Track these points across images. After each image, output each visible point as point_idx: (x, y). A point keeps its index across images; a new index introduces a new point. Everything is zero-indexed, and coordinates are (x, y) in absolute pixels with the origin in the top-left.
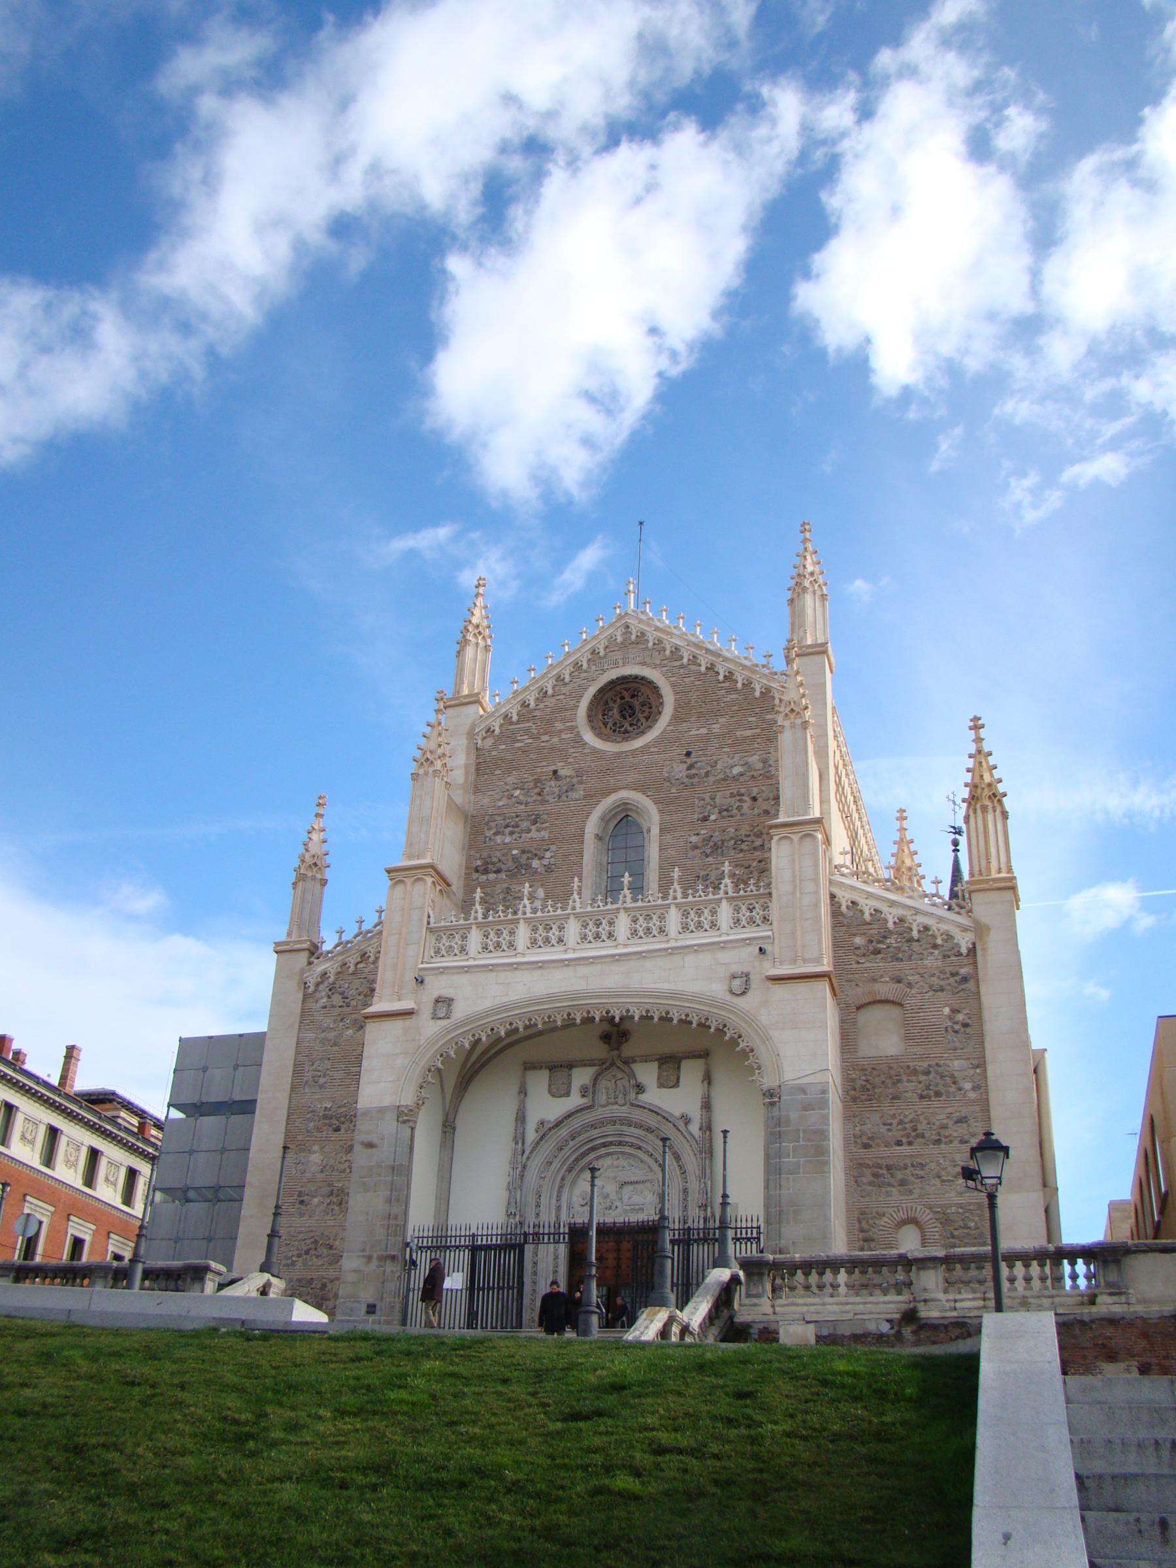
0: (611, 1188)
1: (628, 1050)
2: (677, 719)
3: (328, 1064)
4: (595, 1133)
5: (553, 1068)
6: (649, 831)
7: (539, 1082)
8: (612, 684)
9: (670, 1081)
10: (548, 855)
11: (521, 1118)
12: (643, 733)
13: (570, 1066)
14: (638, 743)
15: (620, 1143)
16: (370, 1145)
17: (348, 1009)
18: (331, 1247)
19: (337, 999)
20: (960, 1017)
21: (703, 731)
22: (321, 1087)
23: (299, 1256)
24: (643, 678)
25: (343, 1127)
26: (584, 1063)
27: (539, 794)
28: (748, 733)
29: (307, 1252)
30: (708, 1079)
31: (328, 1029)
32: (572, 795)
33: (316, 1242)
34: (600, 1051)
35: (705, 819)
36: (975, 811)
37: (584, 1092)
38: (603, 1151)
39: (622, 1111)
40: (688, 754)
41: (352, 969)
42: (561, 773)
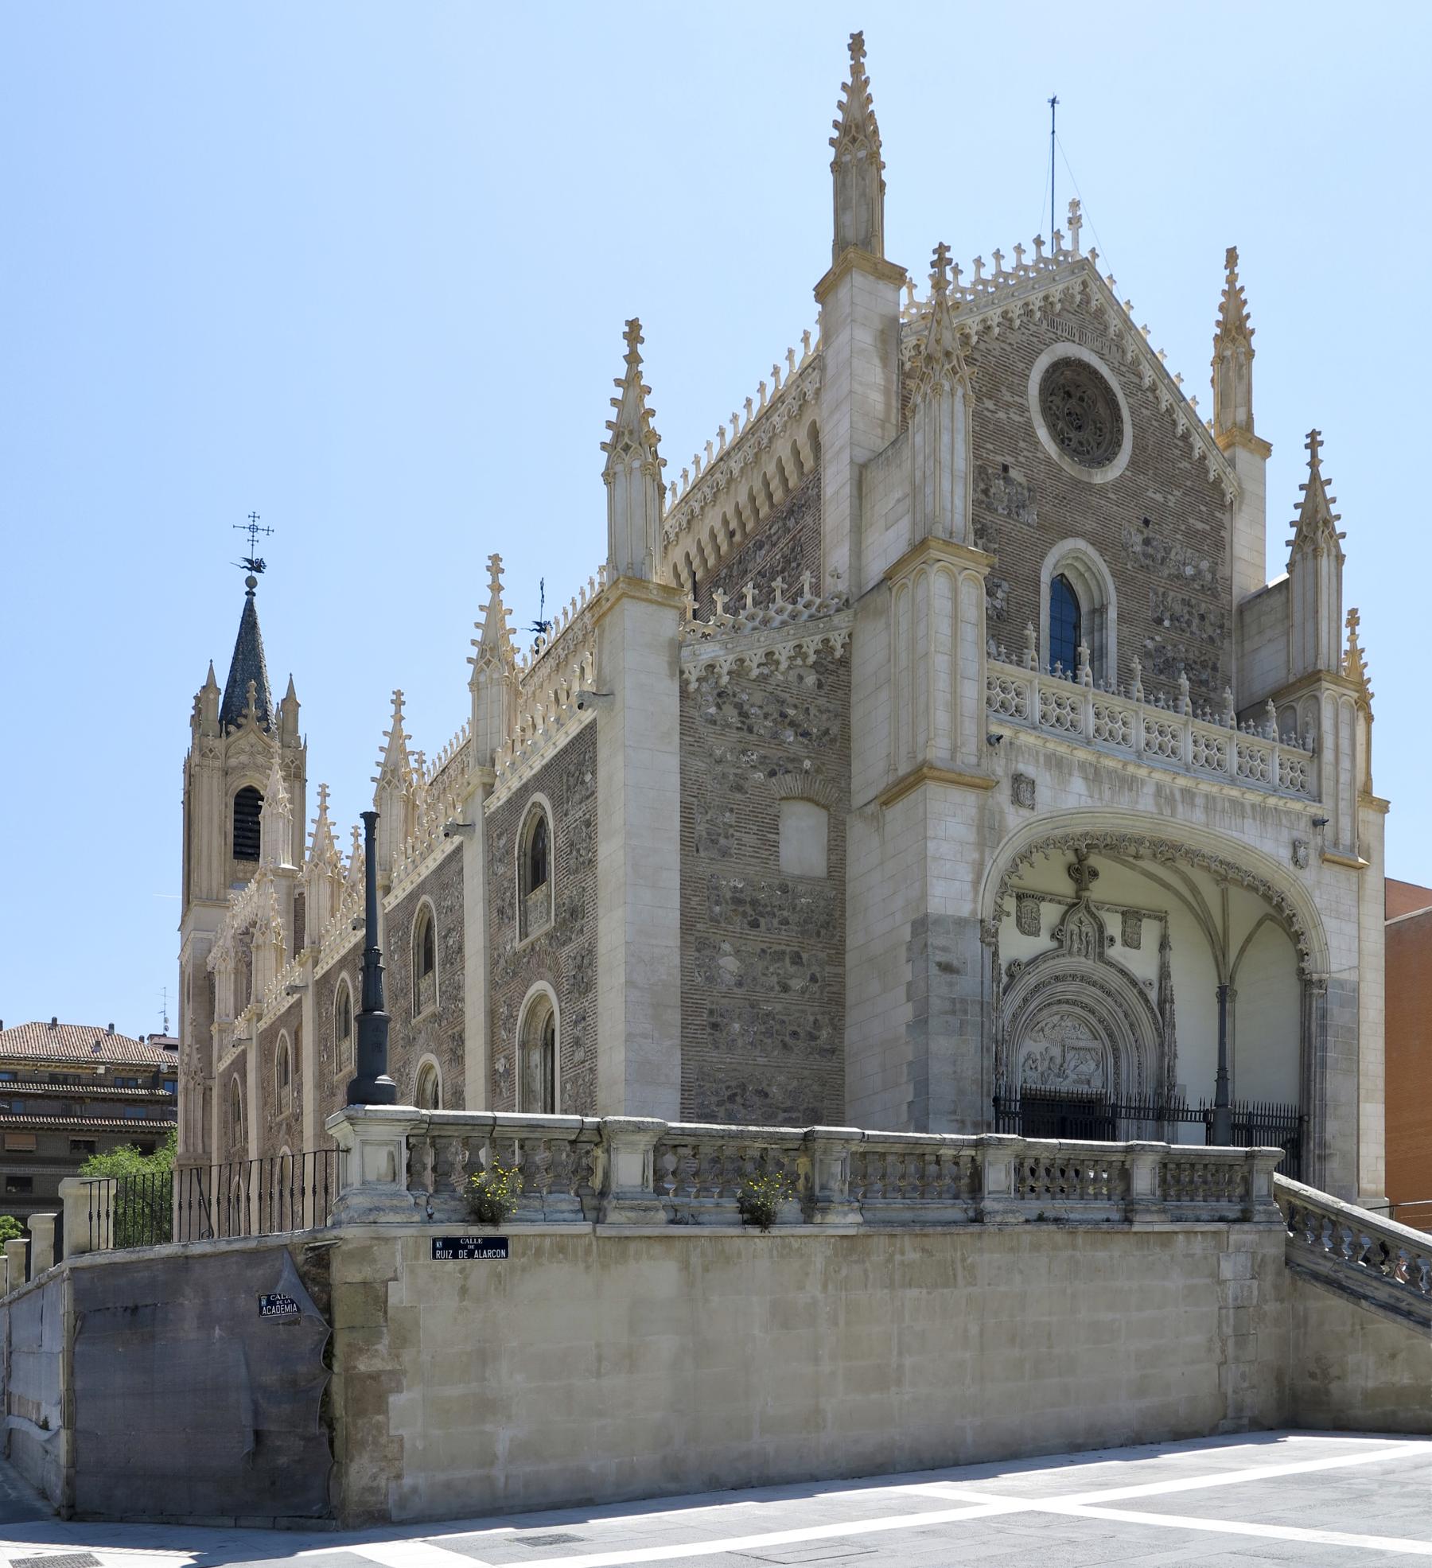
3: (729, 817)
17: (752, 738)
18: (766, 1095)
19: (733, 718)
22: (725, 853)
23: (720, 1104)
25: (762, 921)
29: (732, 1098)
31: (719, 762)
33: (743, 1087)
41: (755, 673)
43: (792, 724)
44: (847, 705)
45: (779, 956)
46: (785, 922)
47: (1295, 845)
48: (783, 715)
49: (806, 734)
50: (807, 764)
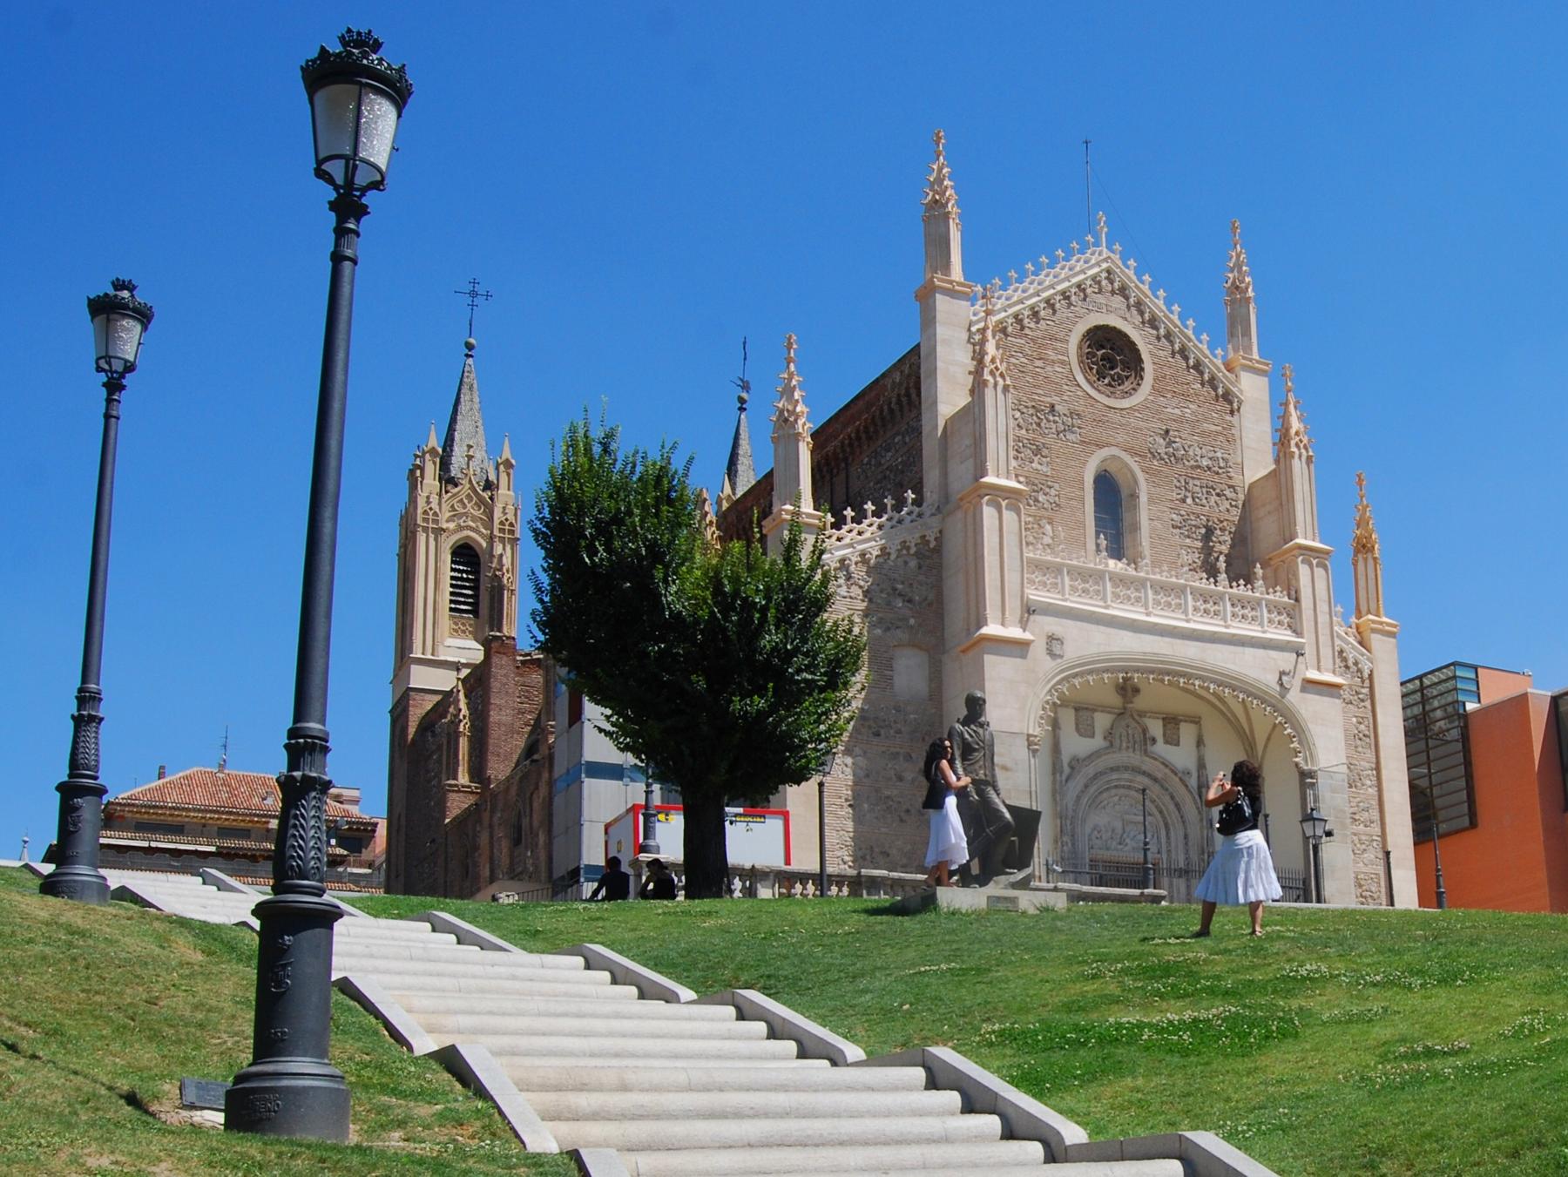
0: (1118, 825)
1: (1140, 703)
2: (1156, 390)
4: (1115, 776)
5: (1076, 709)
6: (1134, 496)
7: (1068, 718)
8: (1098, 328)
9: (1172, 740)
10: (1053, 492)
11: (1056, 749)
12: (1128, 394)
13: (1094, 710)
14: (1126, 403)
15: (1129, 787)
16: (1005, 768)
20: (1362, 727)
21: (1177, 411)
24: (1126, 336)
26: (1105, 709)
27: (1039, 425)
28: (1213, 428)
30: (1200, 742)
32: (1070, 437)
34: (1115, 700)
35: (1183, 501)
36: (1366, 560)
37: (1109, 735)
38: (1113, 792)
39: (1135, 758)
40: (1167, 432)
42: (1057, 408)
43: (900, 595)
44: (940, 579)
45: (895, 756)
46: (899, 732)
47: (1282, 673)
48: (895, 589)
49: (909, 601)
50: (912, 621)
